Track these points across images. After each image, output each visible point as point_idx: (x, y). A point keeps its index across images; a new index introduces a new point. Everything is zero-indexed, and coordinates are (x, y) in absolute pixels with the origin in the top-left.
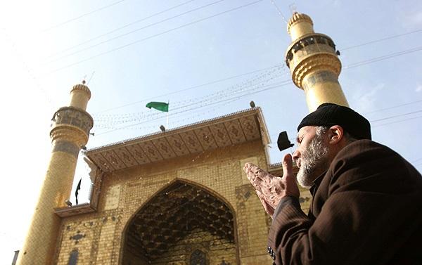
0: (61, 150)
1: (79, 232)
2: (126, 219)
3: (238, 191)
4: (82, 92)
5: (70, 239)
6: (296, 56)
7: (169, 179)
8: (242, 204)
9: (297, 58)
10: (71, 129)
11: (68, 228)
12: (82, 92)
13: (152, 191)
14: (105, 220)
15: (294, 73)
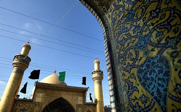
0: (20, 73)
1: (24, 108)
2: (44, 107)
3: (77, 105)
4: (28, 48)
5: (20, 110)
6: (96, 74)
7: (59, 97)
8: (77, 109)
9: (96, 75)
10: (24, 64)
11: (19, 105)
12: (28, 48)
13: (53, 99)
14: (36, 105)
15: (93, 78)
